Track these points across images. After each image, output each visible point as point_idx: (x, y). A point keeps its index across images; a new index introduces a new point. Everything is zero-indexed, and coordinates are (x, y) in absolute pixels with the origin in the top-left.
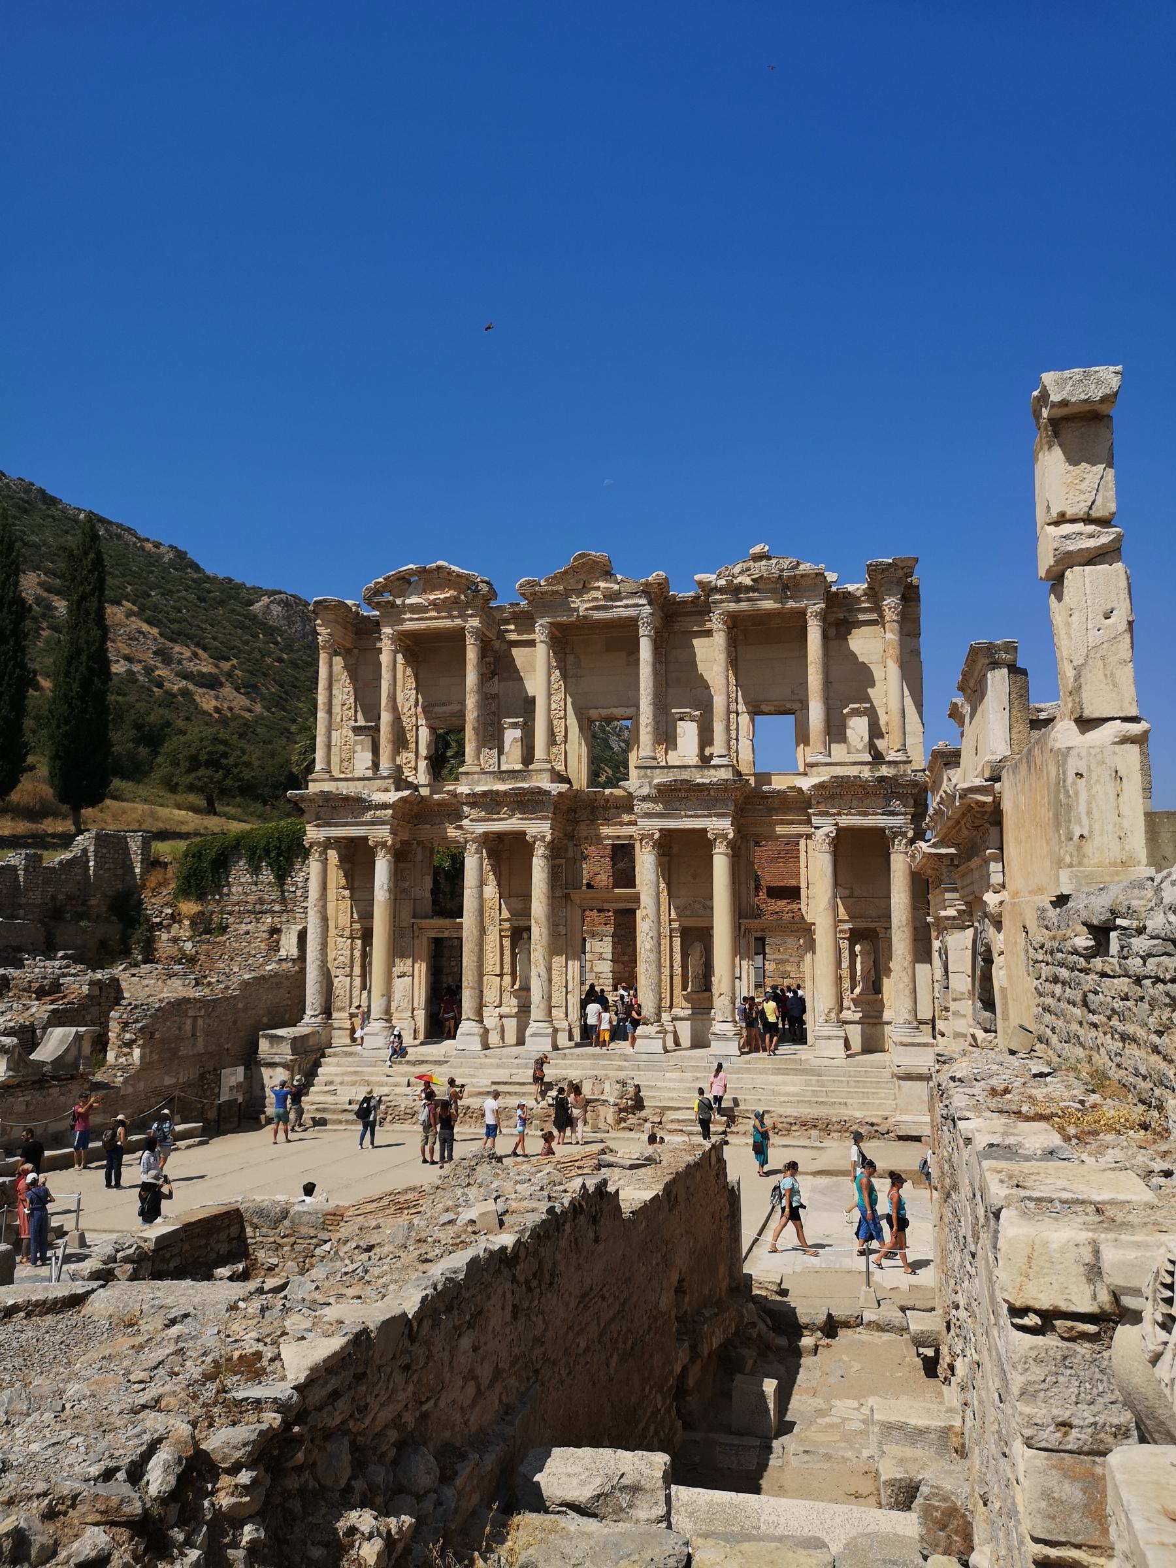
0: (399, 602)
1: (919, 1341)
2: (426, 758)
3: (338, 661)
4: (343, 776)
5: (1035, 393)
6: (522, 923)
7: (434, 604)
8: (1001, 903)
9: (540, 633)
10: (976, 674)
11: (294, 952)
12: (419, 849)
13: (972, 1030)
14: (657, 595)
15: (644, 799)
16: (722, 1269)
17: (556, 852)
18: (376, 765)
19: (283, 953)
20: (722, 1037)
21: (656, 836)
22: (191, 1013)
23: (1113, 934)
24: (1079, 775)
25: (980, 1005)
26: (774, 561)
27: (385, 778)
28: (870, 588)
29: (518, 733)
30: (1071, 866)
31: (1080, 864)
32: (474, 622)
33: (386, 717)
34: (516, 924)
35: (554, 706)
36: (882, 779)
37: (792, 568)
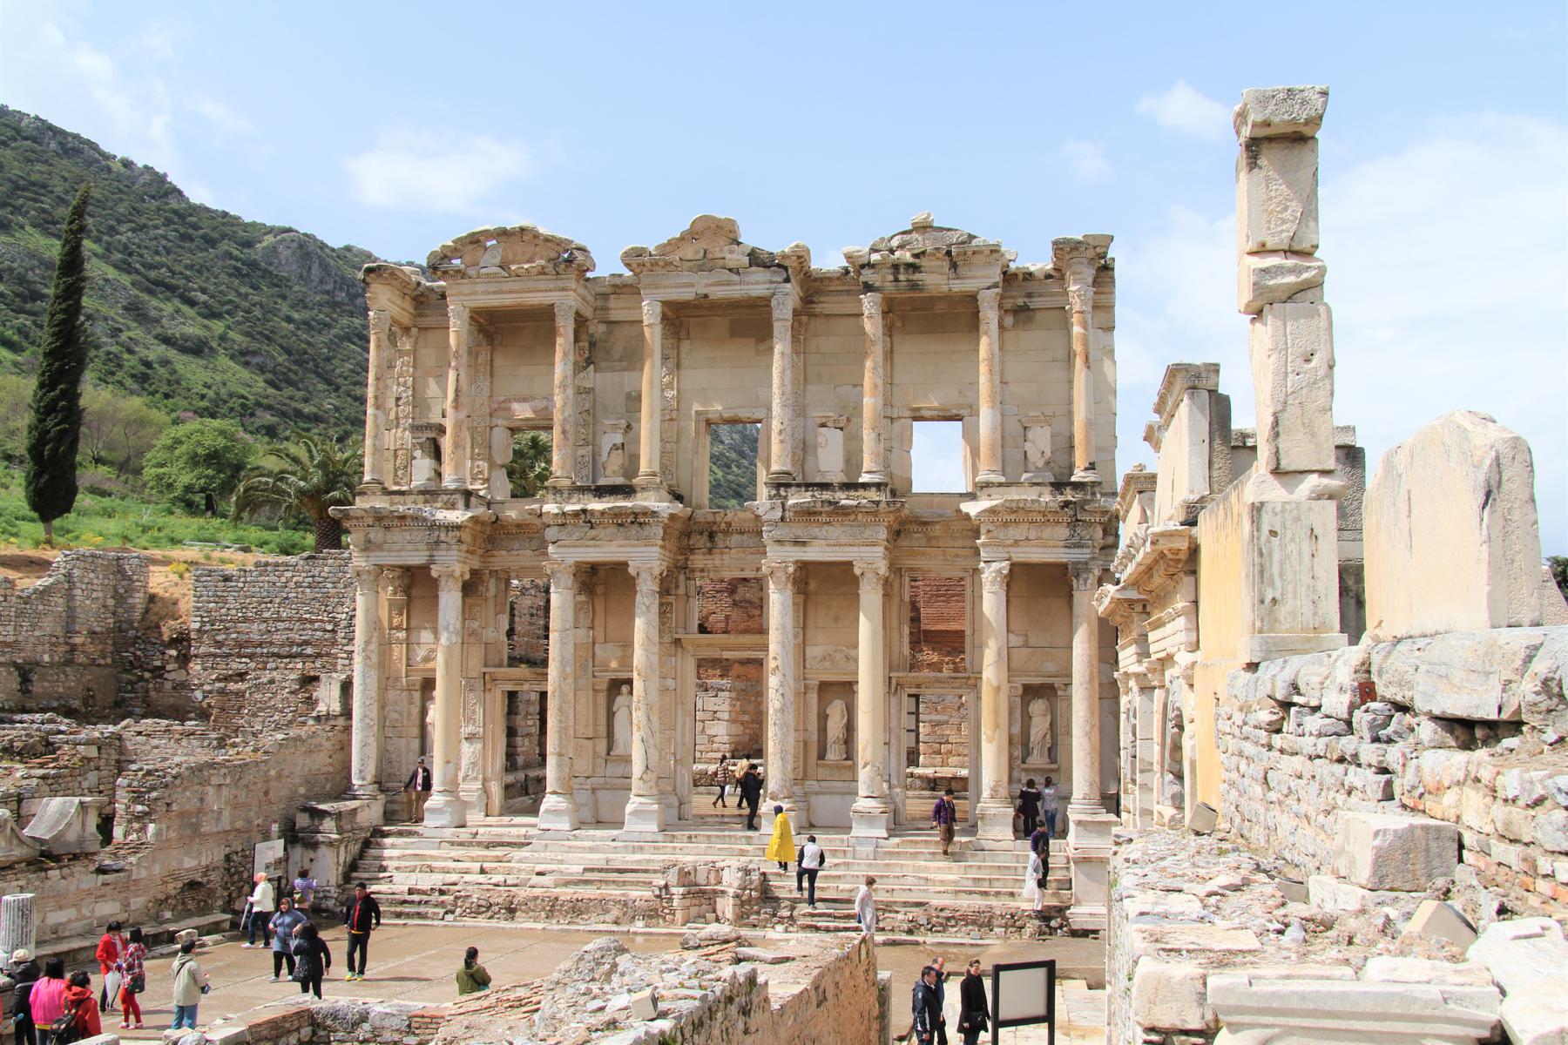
0: (471, 271)
4: (396, 488)
8: (1194, 664)
11: (336, 707)
12: (493, 581)
17: (666, 587)
19: (322, 708)
20: (867, 817)
21: (791, 570)
22: (215, 781)
34: (613, 676)
37: (963, 243)
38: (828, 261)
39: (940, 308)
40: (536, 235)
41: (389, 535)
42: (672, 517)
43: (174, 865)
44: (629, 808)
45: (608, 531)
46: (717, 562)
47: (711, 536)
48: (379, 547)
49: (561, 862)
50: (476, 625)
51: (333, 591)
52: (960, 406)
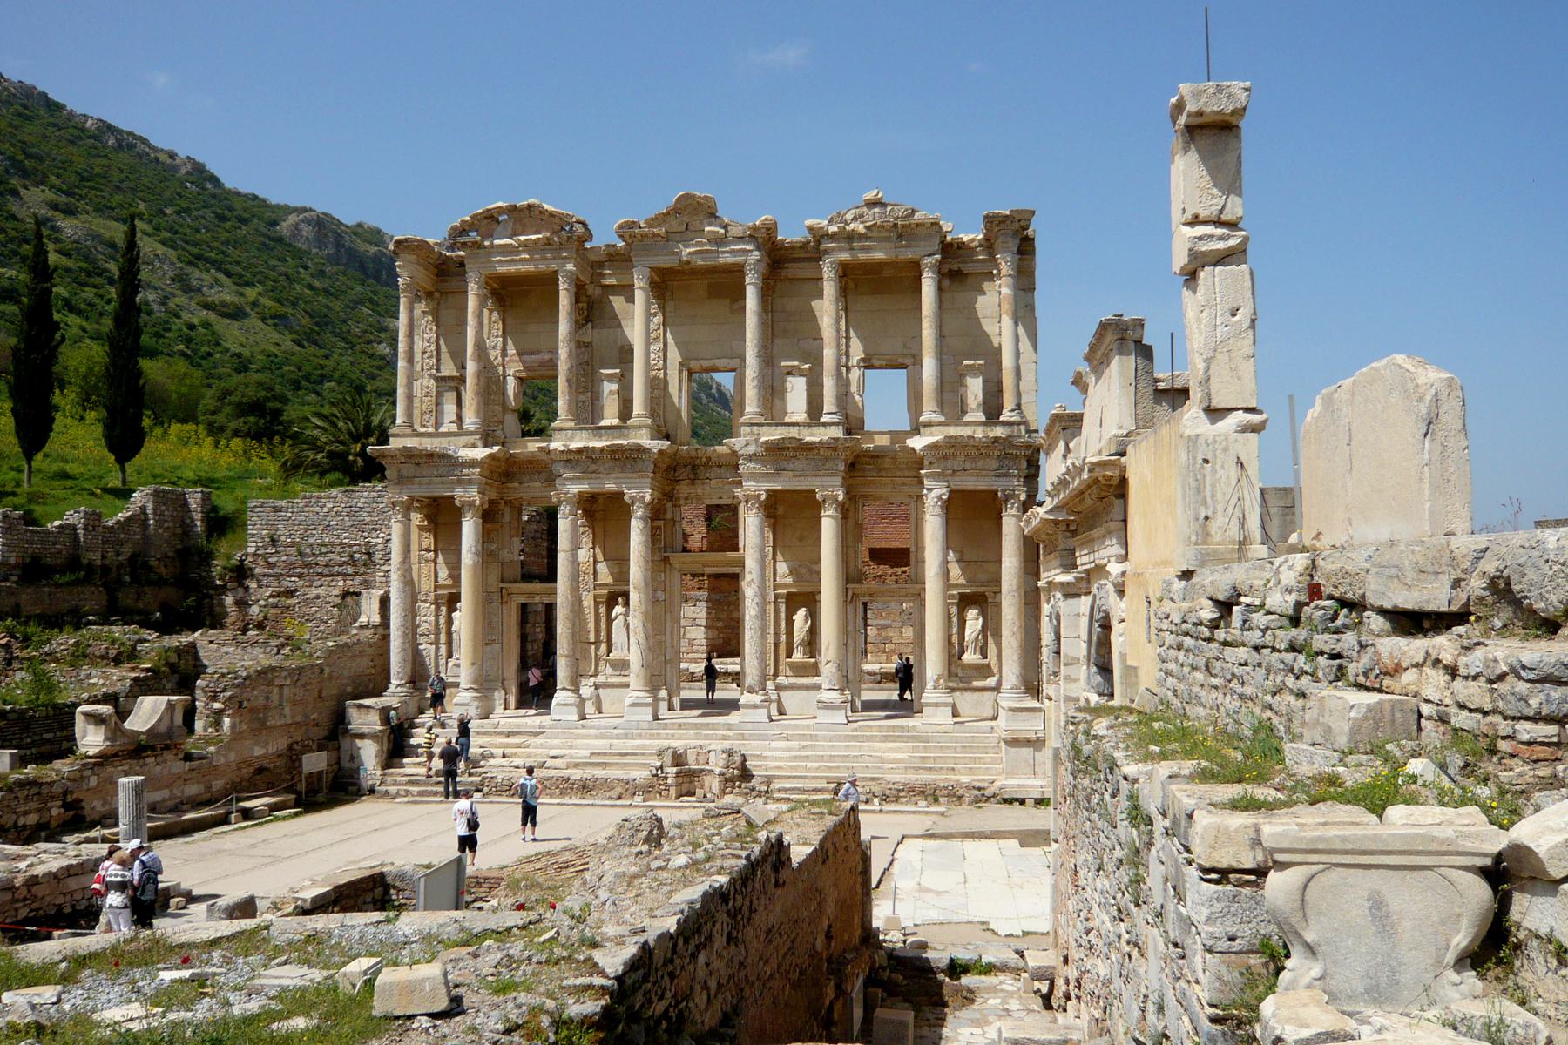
1: (1039, 975)
4: (423, 430)
5: (1174, 100)
7: (525, 245)
8: (1124, 573)
9: (639, 281)
11: (376, 619)
12: (507, 509)
13: (1085, 694)
15: (750, 458)
16: (857, 920)
17: (656, 514)
19: (363, 619)
21: (763, 497)
23: (1235, 609)
24: (1206, 461)
25: (1094, 669)
27: (472, 434)
28: (987, 239)
29: (615, 387)
31: (1205, 543)
32: (570, 267)
33: (471, 367)
35: (652, 356)
36: (996, 440)
38: (791, 234)
39: (887, 273)
40: (543, 212)
43: (246, 753)
46: (699, 492)
47: (694, 468)
49: (571, 747)
50: (493, 547)
52: (905, 355)
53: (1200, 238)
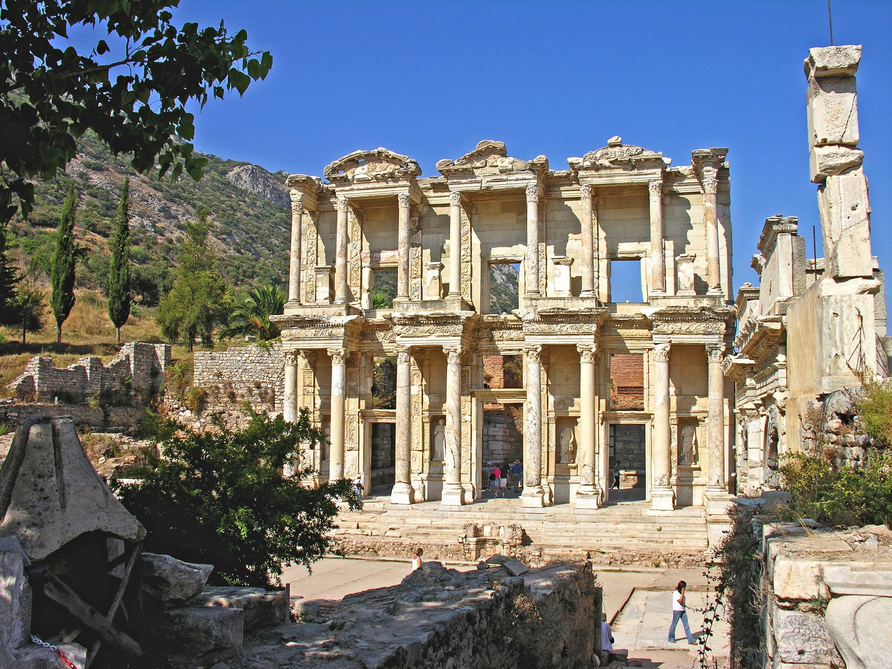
0: (350, 177)
2: (368, 291)
3: (307, 219)
4: (308, 304)
6: (438, 413)
10: (769, 240)
12: (363, 358)
14: (540, 170)
15: (530, 322)
17: (465, 360)
18: (332, 297)
21: (539, 350)
24: (835, 314)
26: (625, 149)
30: (830, 374)
31: (836, 374)
35: (463, 253)
36: (703, 309)
37: (638, 154)
40: (387, 156)
41: (303, 331)
42: (468, 318)
44: (443, 492)
45: (431, 327)
48: (298, 339)
51: (271, 365)
53: (827, 156)
